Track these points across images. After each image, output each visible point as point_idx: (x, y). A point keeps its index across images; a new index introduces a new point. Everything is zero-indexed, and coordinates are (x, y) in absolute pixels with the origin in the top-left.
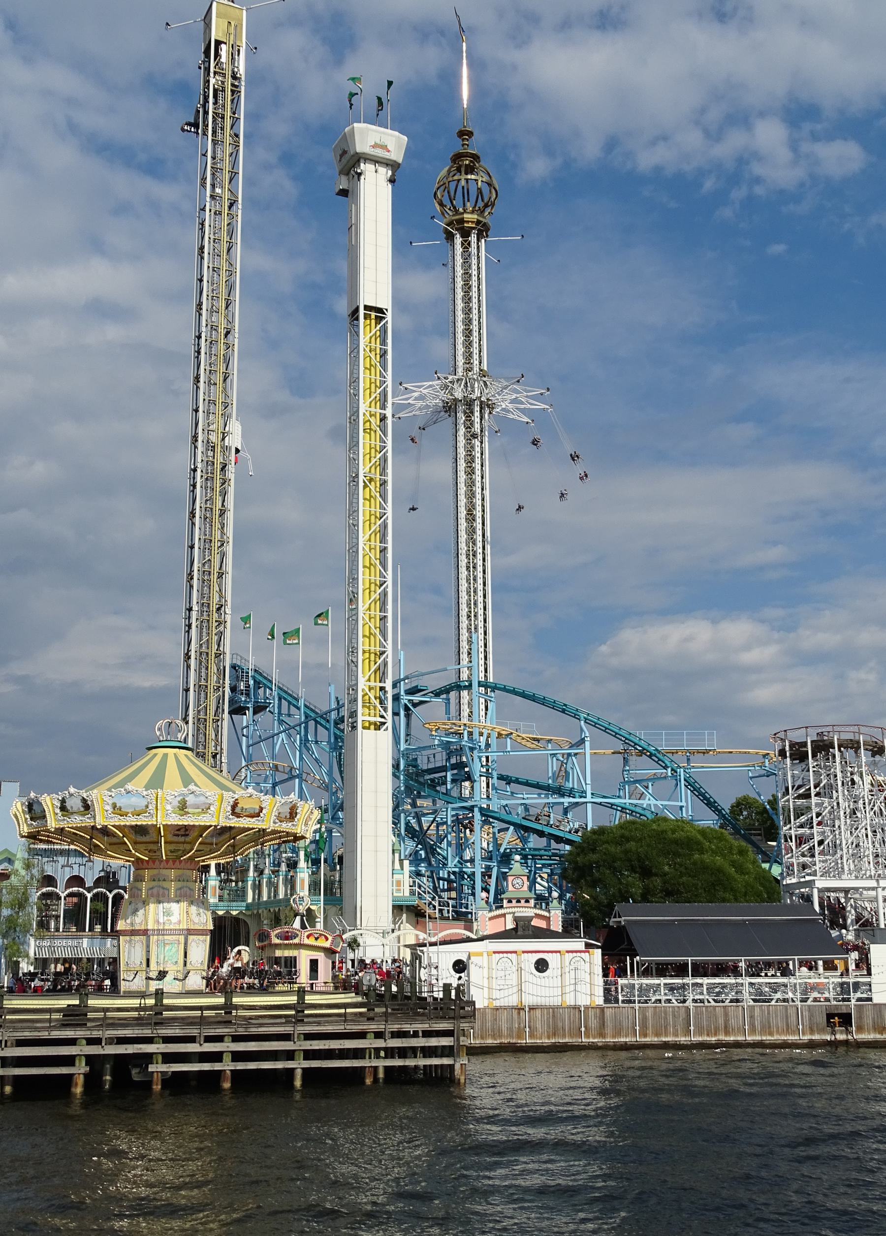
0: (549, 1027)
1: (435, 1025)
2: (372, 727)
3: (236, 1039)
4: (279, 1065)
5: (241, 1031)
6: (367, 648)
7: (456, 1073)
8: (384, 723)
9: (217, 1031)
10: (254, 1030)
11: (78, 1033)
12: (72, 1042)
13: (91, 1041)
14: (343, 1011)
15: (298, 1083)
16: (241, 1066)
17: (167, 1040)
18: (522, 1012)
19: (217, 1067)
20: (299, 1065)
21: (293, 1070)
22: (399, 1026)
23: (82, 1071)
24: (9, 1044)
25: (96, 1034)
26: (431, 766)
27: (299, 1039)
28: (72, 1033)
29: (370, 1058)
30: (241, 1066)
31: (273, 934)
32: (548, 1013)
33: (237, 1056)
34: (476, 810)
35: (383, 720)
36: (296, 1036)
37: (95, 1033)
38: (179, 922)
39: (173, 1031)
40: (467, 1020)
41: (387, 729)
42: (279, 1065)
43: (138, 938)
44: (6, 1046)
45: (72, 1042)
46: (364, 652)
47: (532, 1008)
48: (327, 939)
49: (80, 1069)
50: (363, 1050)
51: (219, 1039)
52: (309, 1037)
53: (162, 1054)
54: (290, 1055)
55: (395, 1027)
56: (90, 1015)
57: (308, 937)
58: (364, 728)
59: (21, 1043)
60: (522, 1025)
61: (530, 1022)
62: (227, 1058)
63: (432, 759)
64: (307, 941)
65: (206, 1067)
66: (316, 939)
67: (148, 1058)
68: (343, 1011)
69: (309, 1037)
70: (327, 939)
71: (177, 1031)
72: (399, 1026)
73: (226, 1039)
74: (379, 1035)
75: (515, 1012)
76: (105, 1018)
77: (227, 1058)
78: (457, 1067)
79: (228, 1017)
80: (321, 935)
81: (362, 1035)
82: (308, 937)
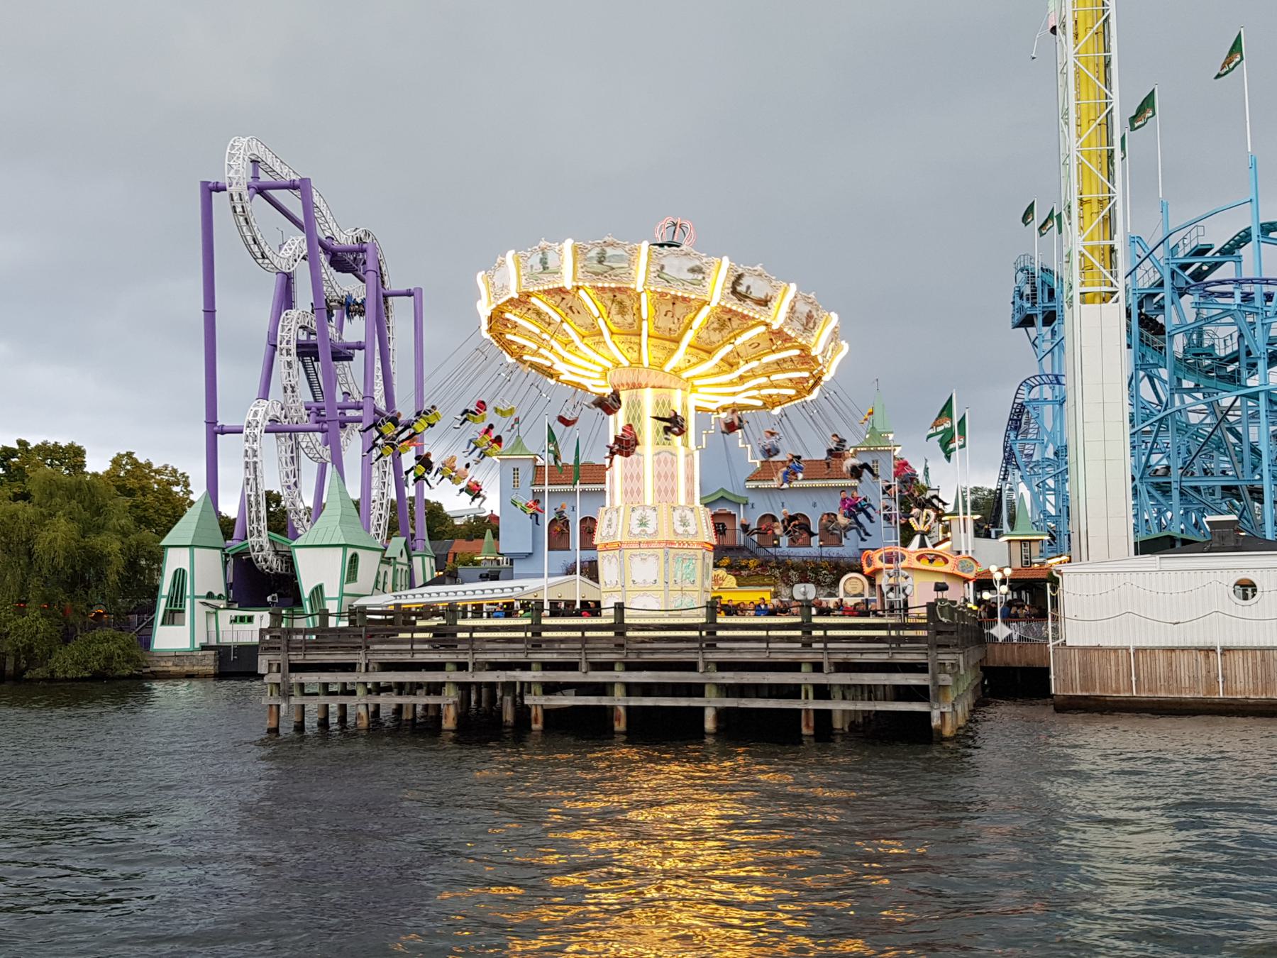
0: (1255, 674)
1: (898, 656)
2: (1098, 299)
3: (629, 667)
4: (683, 702)
5: (632, 658)
6: (1086, 197)
7: (933, 724)
8: (1114, 293)
9: (603, 656)
10: (647, 657)
11: (443, 656)
12: (439, 667)
13: (462, 666)
14: (764, 633)
15: (709, 725)
16: (635, 702)
17: (546, 666)
18: (1211, 654)
19: (605, 701)
20: (711, 704)
21: (701, 710)
22: (845, 656)
23: (450, 701)
24: (371, 667)
25: (462, 658)
26: (1229, 351)
27: (706, 670)
28: (436, 656)
29: (807, 698)
30: (635, 702)
31: (876, 556)
32: (1254, 657)
33: (630, 689)
34: (1262, 396)
35: (1113, 289)
36: (701, 665)
37: (461, 656)
38: (657, 532)
39: (549, 656)
40: (947, 650)
41: (1117, 301)
42: (683, 702)
43: (611, 553)
44: (367, 670)
45: (439, 667)
46: (1082, 202)
47: (1225, 650)
48: (946, 561)
49: (449, 699)
50: (798, 686)
51: (609, 666)
52: (723, 666)
53: (541, 683)
54: (696, 690)
55: (840, 657)
56: (460, 635)
57: (919, 558)
58: (1083, 302)
59: (386, 667)
60: (1212, 674)
61: (1224, 669)
62: (619, 691)
63: (1229, 342)
64: (917, 565)
65: (592, 701)
66: (931, 561)
67: (527, 687)
68: (764, 633)
69: (723, 666)
70: (946, 561)
71: (555, 656)
72: (845, 656)
73: (617, 667)
74: (817, 667)
75: (1201, 656)
76: (471, 638)
77: (619, 691)
78: (935, 714)
79: (621, 640)
80: (937, 556)
81: (795, 667)
82: (919, 558)
